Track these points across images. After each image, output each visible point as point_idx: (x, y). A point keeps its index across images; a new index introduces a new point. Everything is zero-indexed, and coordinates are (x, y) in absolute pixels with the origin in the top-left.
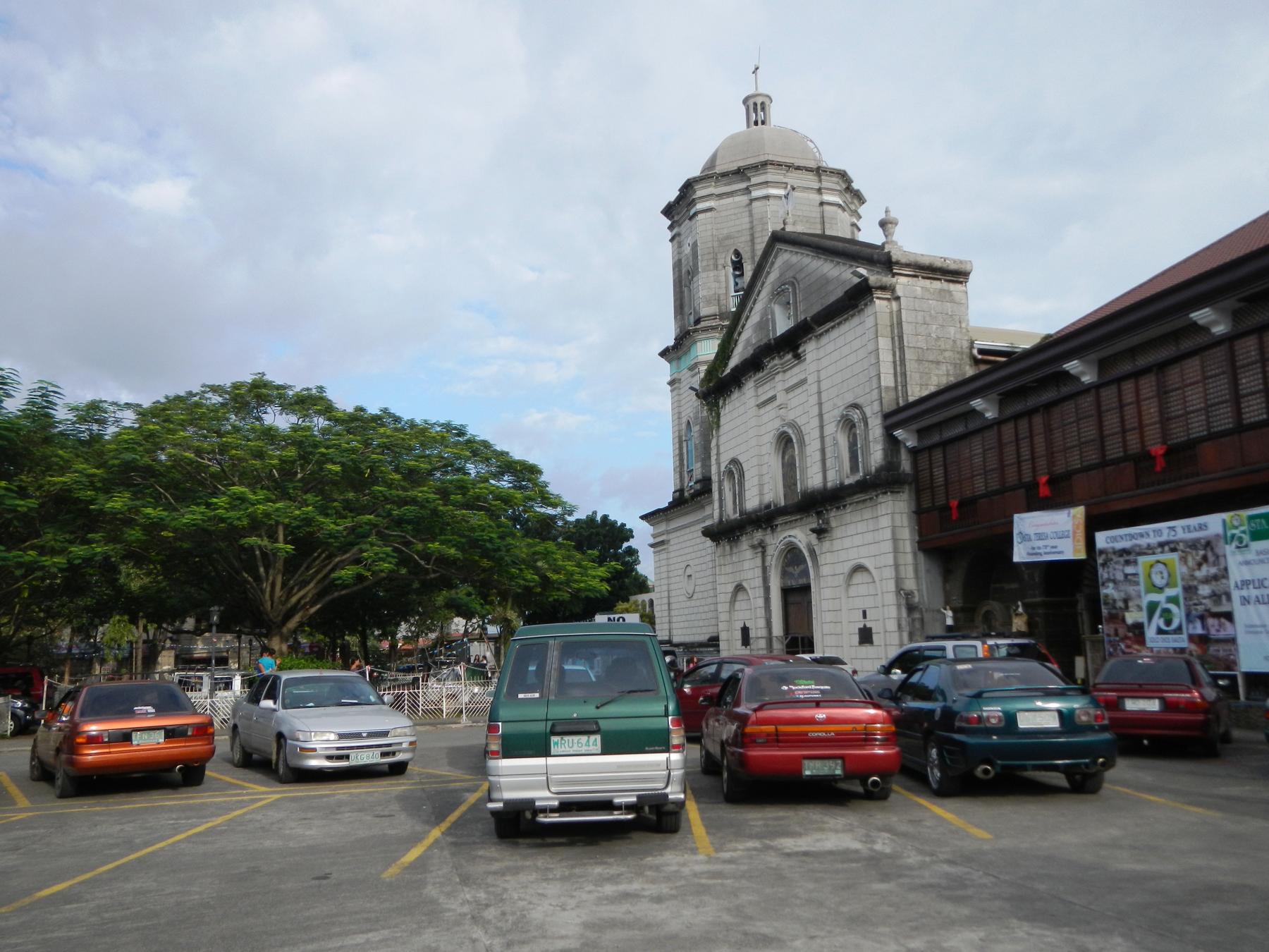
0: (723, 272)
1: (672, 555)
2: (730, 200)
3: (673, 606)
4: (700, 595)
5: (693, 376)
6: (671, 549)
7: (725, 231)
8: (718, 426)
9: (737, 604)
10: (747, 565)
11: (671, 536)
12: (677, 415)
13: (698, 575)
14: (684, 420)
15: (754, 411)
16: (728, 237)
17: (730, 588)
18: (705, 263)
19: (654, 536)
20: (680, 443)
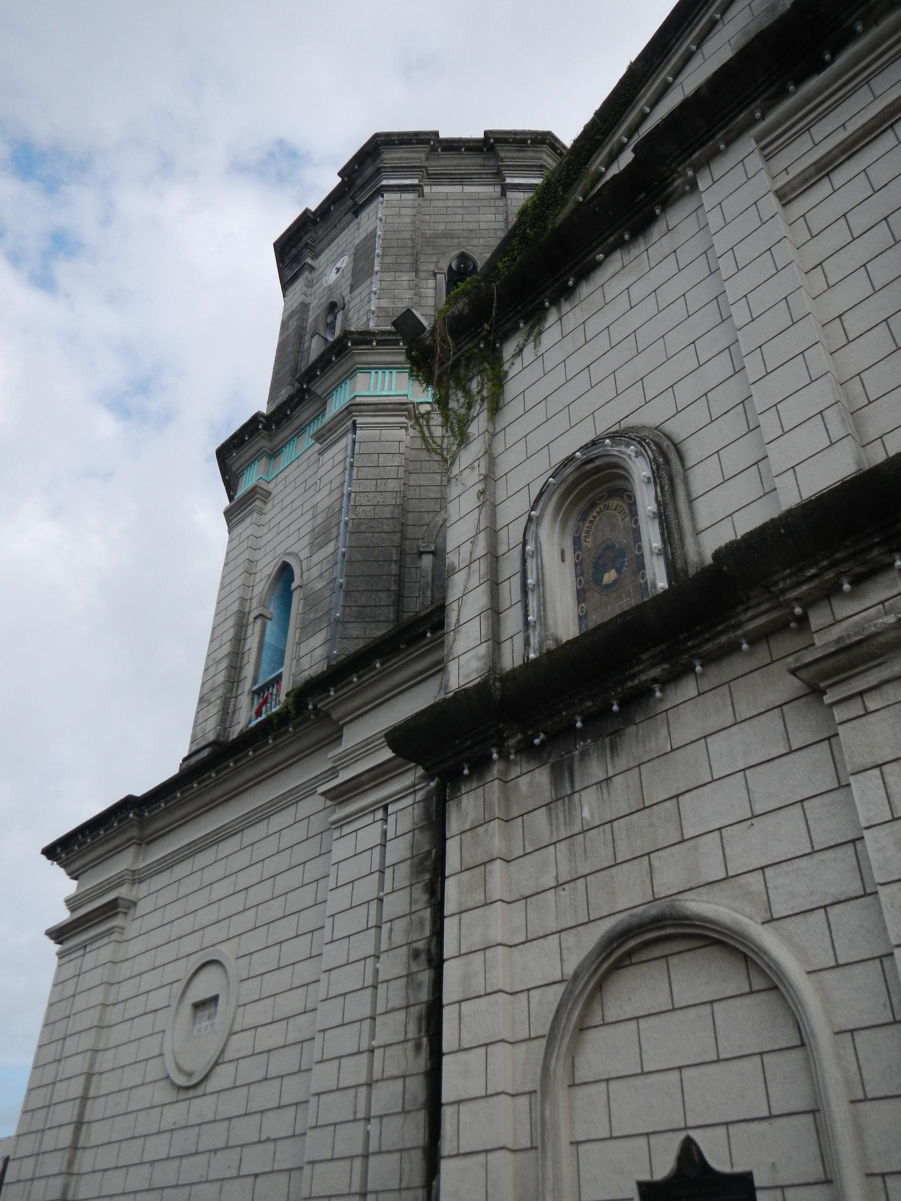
0: (431, 283)
1: (136, 947)
2: (458, 189)
3: (96, 1134)
4: (251, 1070)
5: (321, 453)
6: (134, 928)
7: (442, 227)
8: (495, 408)
9: (603, 1051)
10: (703, 811)
11: (143, 889)
12: (239, 565)
13: (250, 990)
14: (267, 568)
15: (773, 203)
16: (446, 235)
17: (555, 961)
18: (388, 260)
19: (72, 903)
20: (241, 627)
